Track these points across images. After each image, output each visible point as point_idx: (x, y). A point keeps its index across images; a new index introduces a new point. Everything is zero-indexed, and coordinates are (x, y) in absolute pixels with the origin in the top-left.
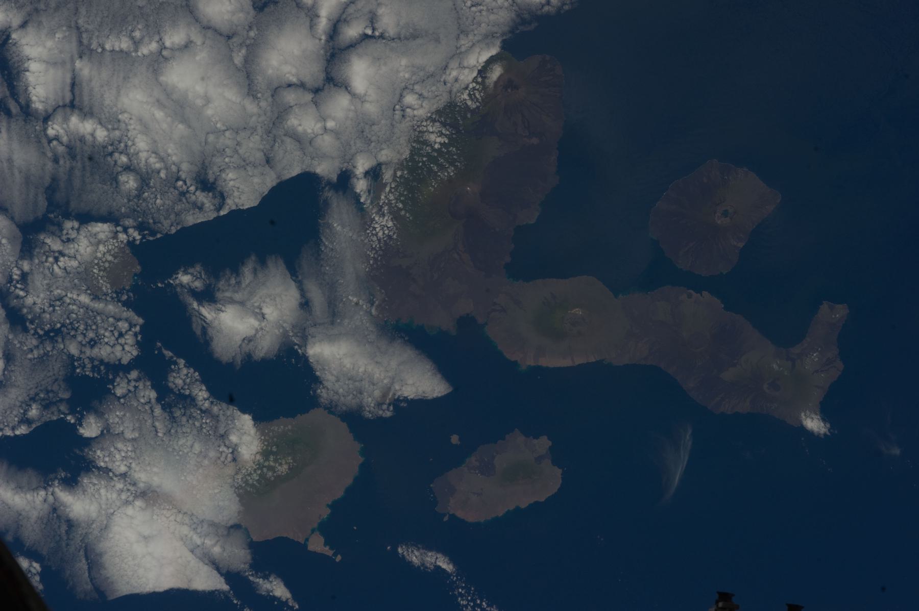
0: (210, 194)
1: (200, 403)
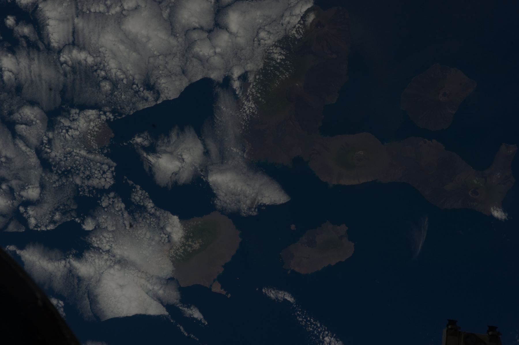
0: (152, 92)
1: (149, 210)
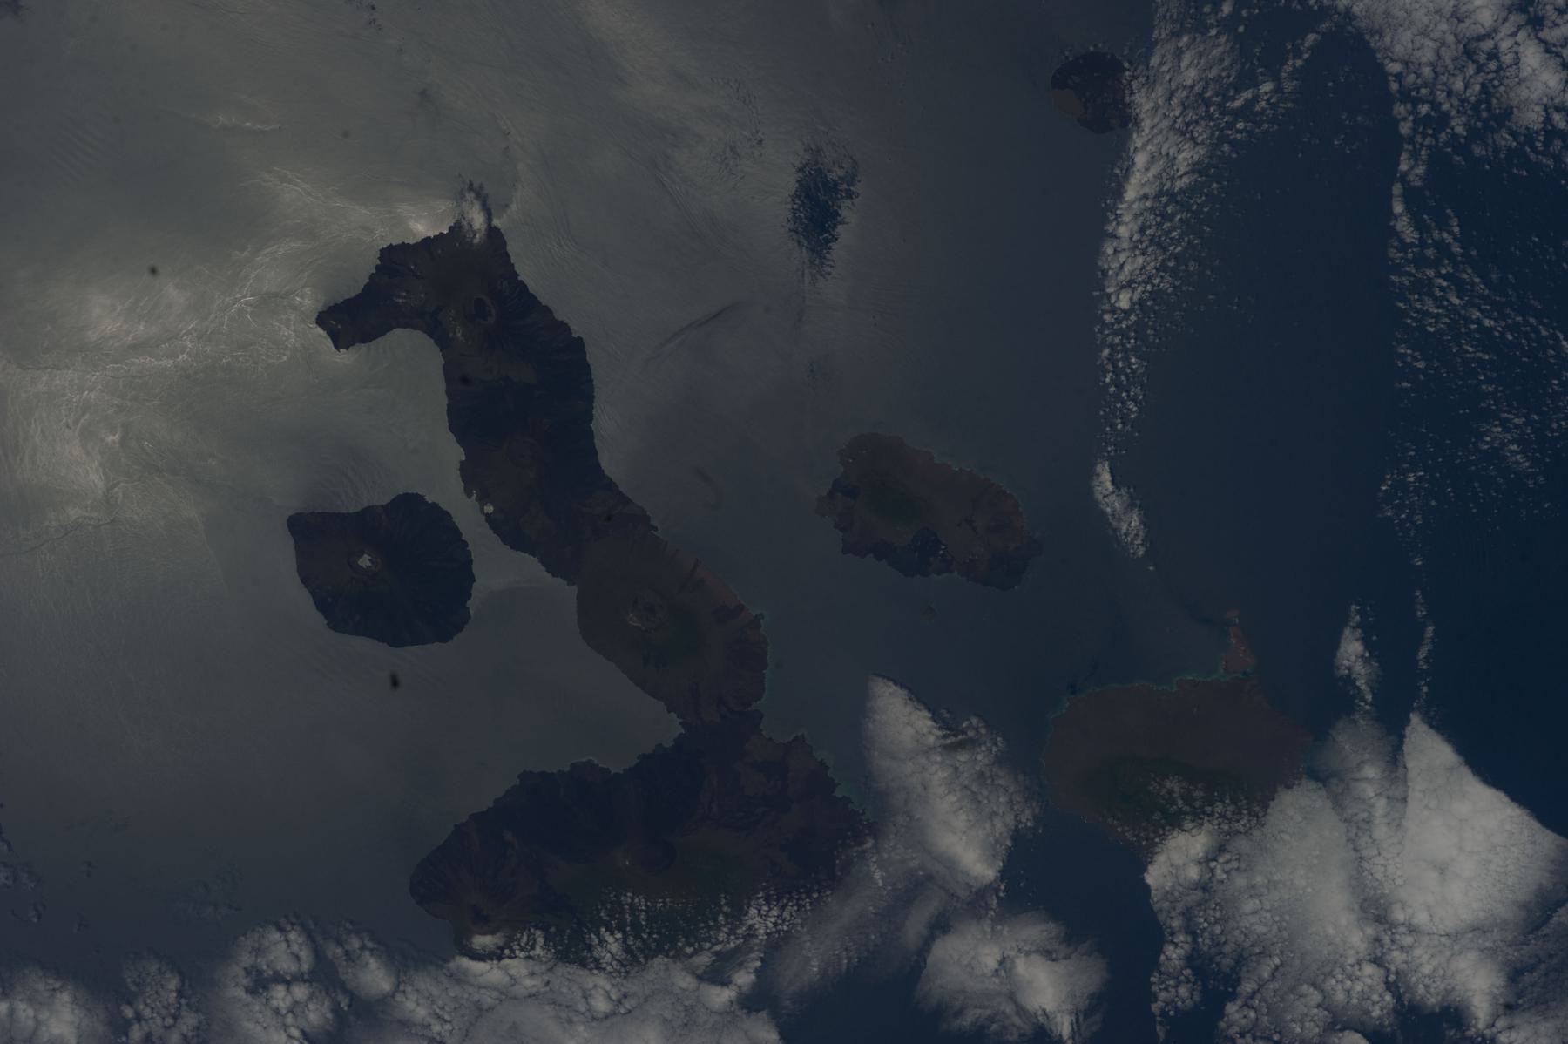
1: (1186, 946)
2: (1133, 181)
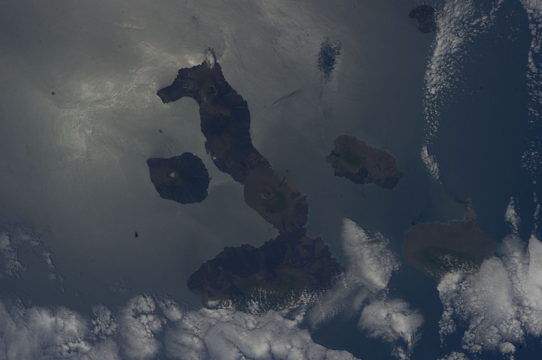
1: (451, 312)
2: (437, 50)
